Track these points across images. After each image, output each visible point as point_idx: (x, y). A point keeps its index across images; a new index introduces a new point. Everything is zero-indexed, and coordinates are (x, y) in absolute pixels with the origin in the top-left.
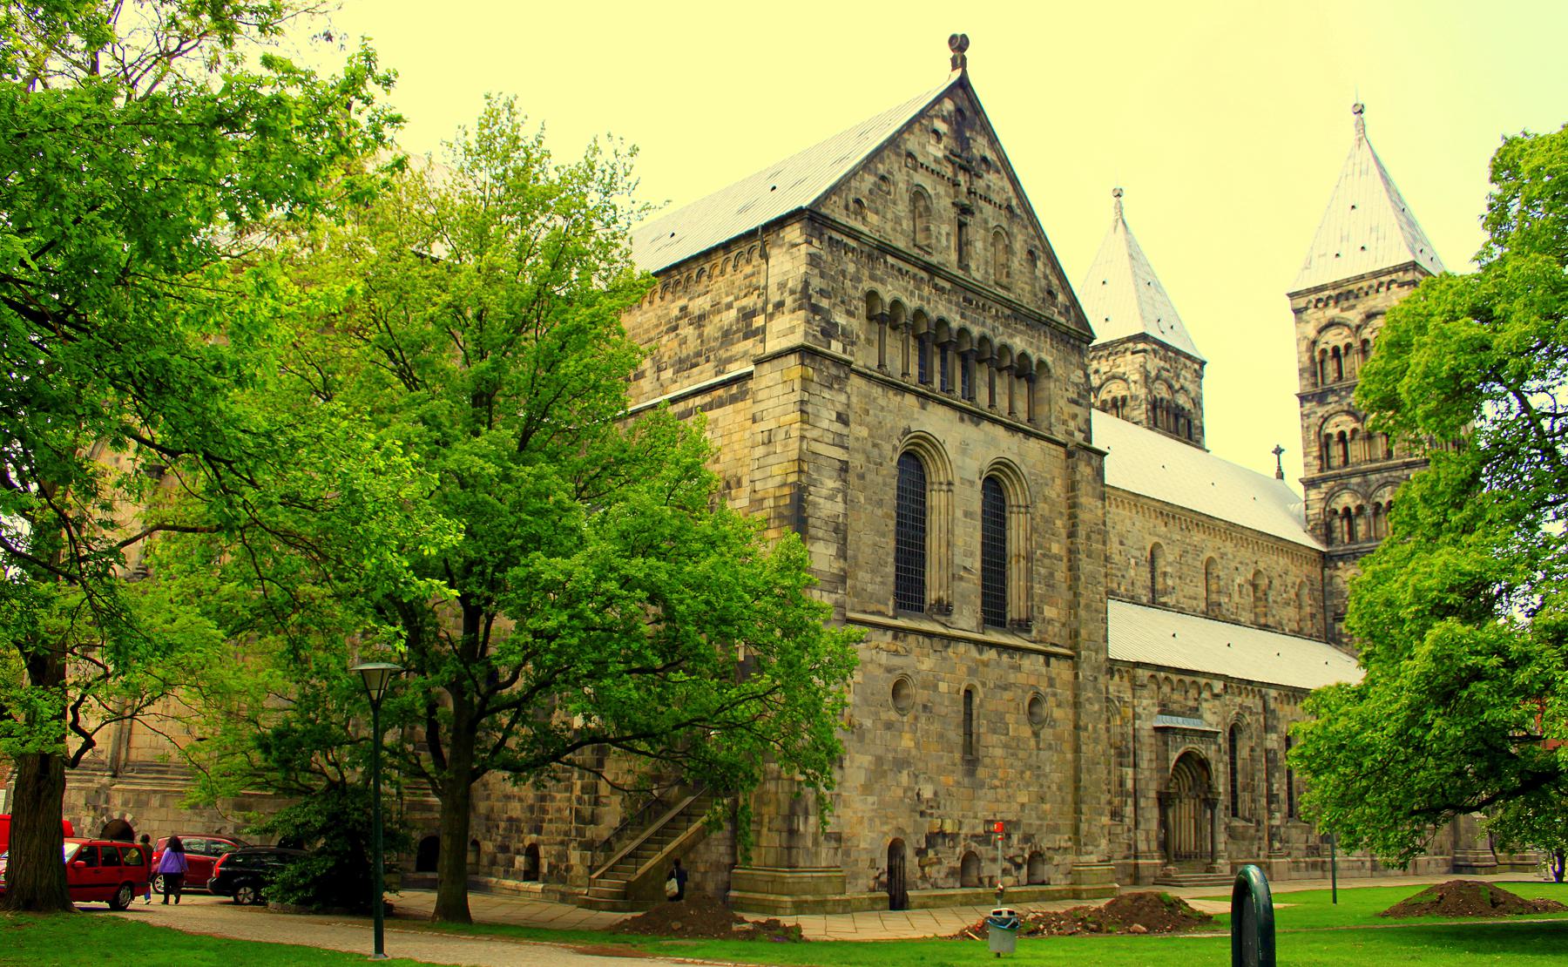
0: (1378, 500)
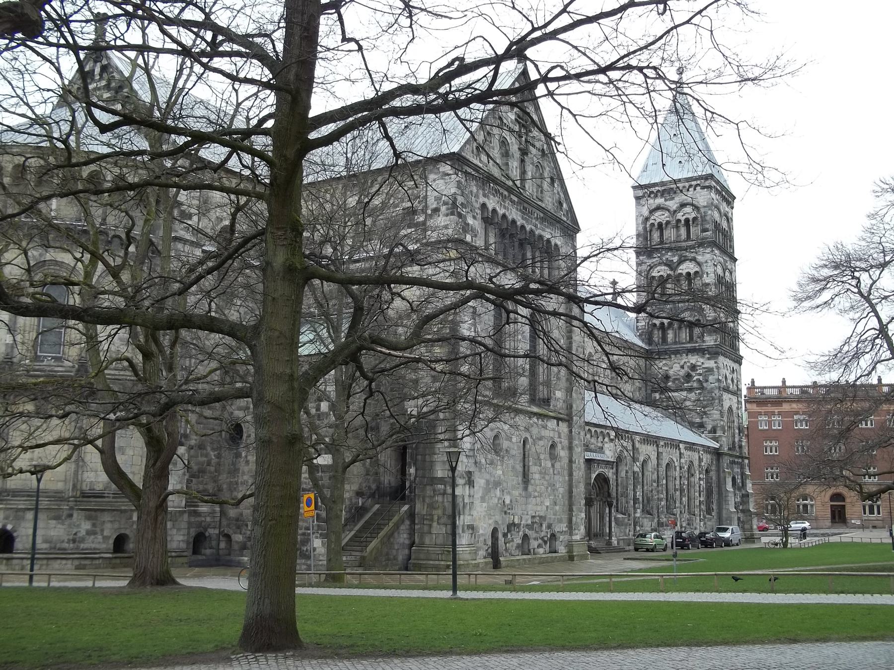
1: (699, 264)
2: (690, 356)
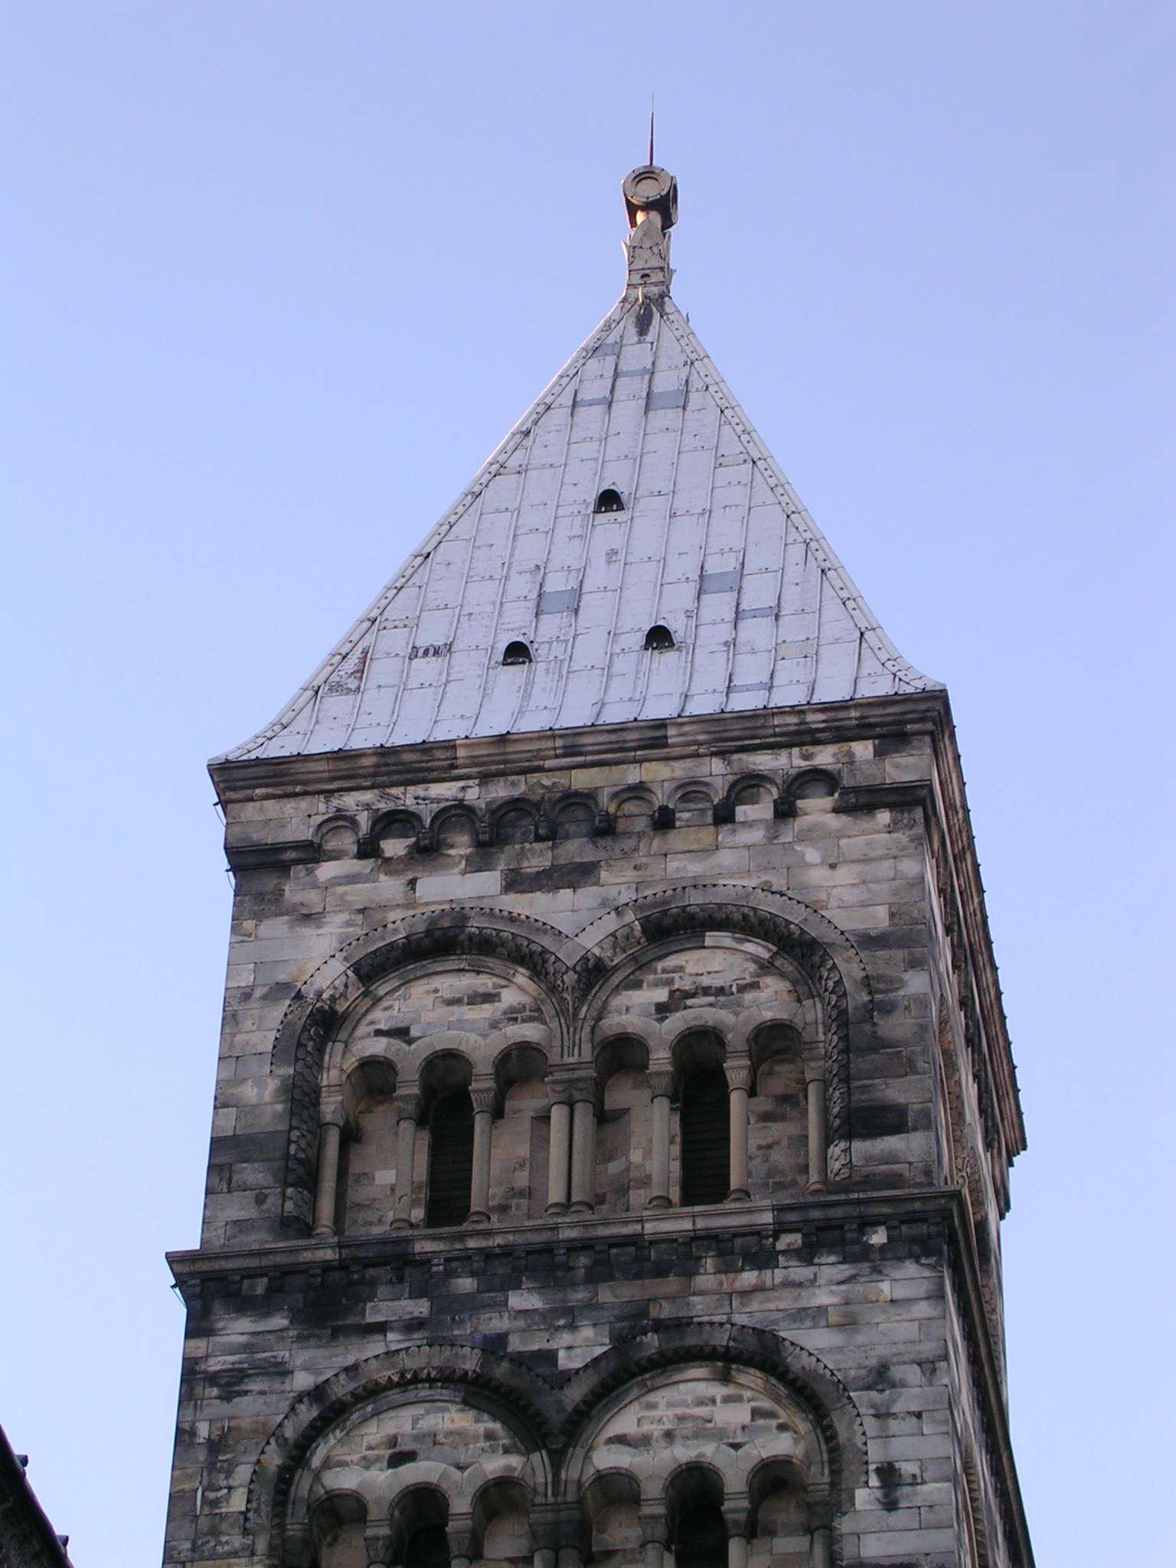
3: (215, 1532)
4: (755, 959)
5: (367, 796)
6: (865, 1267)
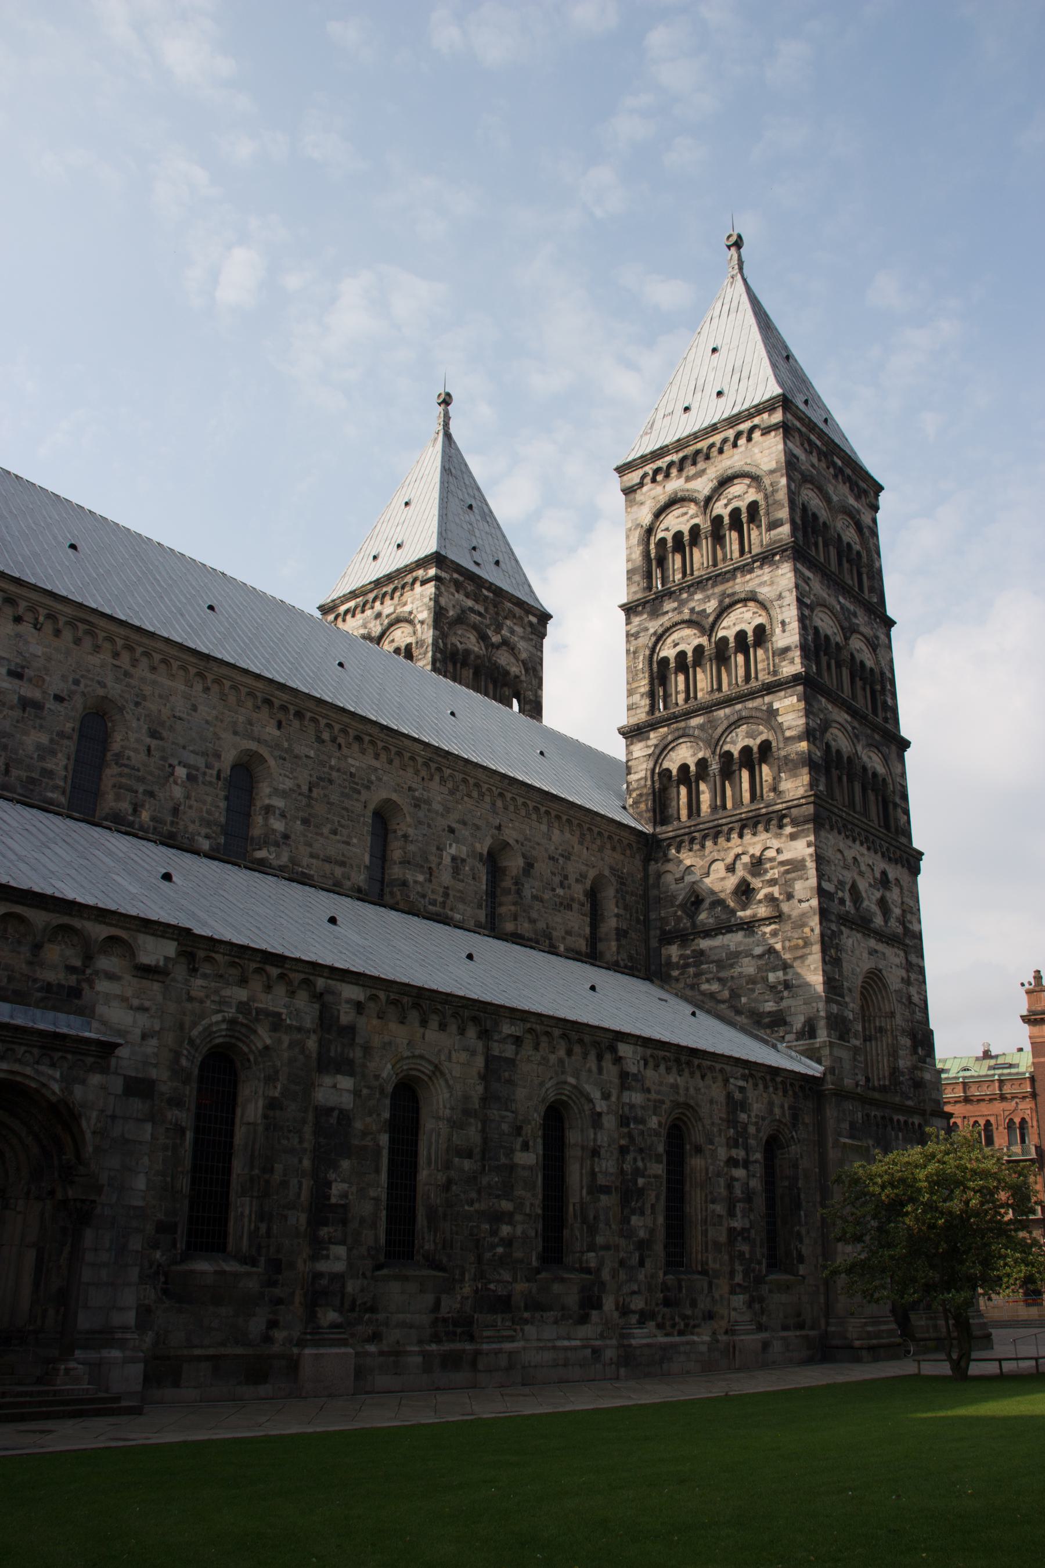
0: (726, 748)
1: (763, 606)
2: (748, 837)
3: (637, 675)
4: (746, 484)
5: (651, 466)
6: (775, 567)
